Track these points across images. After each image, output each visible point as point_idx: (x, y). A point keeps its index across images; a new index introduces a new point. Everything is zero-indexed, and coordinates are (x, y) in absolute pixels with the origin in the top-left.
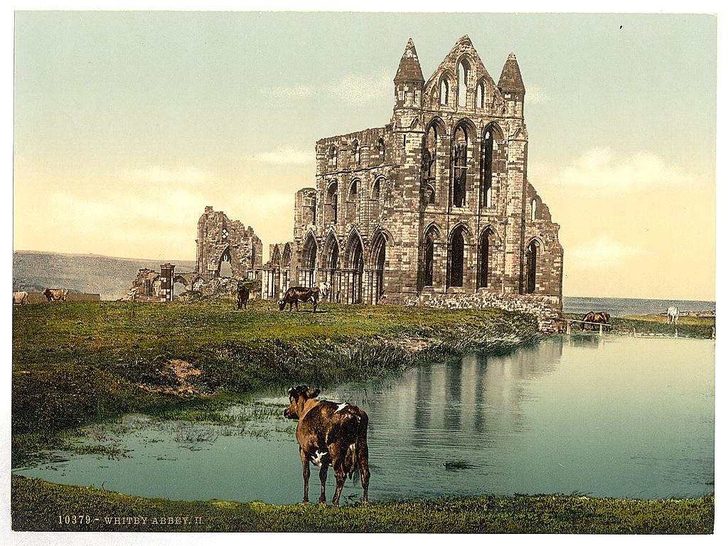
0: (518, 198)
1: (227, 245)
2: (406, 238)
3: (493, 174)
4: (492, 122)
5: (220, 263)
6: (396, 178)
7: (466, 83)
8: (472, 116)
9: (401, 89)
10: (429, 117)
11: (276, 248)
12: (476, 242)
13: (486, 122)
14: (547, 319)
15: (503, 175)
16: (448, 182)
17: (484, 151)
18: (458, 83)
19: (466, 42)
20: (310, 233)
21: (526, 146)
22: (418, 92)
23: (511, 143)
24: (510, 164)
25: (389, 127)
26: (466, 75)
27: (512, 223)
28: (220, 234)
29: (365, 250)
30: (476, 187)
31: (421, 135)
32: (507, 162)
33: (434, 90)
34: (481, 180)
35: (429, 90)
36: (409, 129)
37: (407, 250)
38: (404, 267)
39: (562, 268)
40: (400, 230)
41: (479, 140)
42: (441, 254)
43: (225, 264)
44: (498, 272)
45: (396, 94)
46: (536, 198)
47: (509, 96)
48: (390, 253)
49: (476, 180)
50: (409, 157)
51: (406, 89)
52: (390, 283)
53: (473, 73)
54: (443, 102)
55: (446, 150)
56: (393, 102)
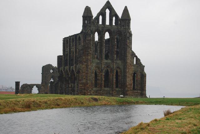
19: (108, 3)
46: (136, 57)
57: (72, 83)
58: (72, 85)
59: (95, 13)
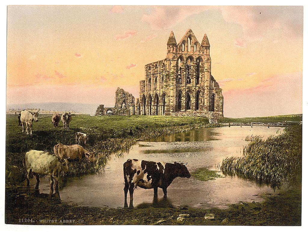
1: (124, 99)
2: (171, 95)
3: (200, 73)
4: (200, 56)
5: (122, 104)
7: (190, 44)
10: (178, 56)
14: (212, 119)
16: (185, 76)
18: (188, 44)
19: (190, 31)
21: (210, 64)
22: (175, 47)
25: (166, 59)
26: (191, 42)
27: (206, 89)
28: (123, 96)
30: (194, 77)
33: (180, 46)
34: (196, 75)
35: (178, 47)
36: (172, 60)
37: (172, 98)
38: (171, 104)
39: (223, 103)
41: (195, 62)
42: (183, 100)
43: (124, 105)
45: (168, 49)
46: (215, 81)
47: (205, 48)
48: (166, 100)
49: (194, 75)
51: (171, 47)
53: (193, 40)
54: (183, 50)
56: (166, 51)
59: (178, 41)
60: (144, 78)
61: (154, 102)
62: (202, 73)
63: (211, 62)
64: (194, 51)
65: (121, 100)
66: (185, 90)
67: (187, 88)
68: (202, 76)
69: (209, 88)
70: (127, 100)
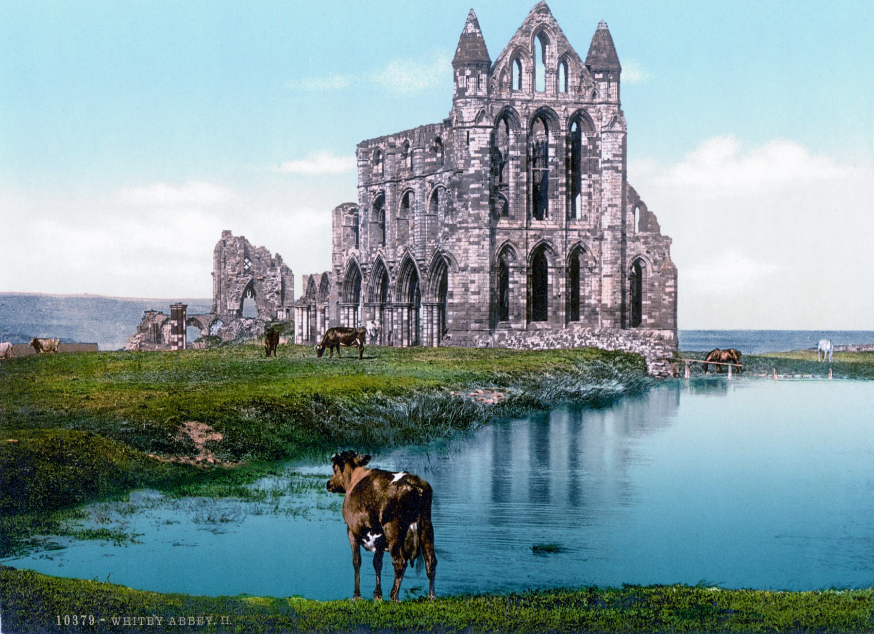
0: (616, 206)
1: (250, 277)
3: (583, 176)
4: (580, 110)
5: (242, 300)
6: (458, 186)
7: (544, 62)
8: (554, 103)
9: (462, 73)
10: (498, 107)
11: (311, 280)
12: (563, 264)
13: (572, 110)
15: (595, 177)
16: (525, 188)
17: (570, 147)
18: (534, 63)
19: (543, 9)
20: (353, 259)
21: (624, 140)
22: (484, 76)
23: (604, 135)
24: (604, 162)
25: (448, 123)
26: (544, 51)
28: (243, 265)
29: (421, 280)
30: (561, 193)
31: (489, 130)
32: (600, 161)
33: (503, 73)
34: (567, 184)
35: (497, 73)
36: (473, 124)
37: (475, 277)
38: (473, 299)
39: (676, 293)
40: (466, 251)
41: (564, 134)
42: (519, 281)
43: (249, 301)
44: (593, 301)
45: (456, 80)
47: (601, 76)
48: (453, 281)
49: (562, 185)
50: (474, 158)
51: (468, 72)
52: (456, 319)
53: (553, 48)
55: (521, 149)
56: (451, 90)
57: (402, 307)
58: (402, 313)
60: (353, 196)
61: (400, 290)
62: (590, 176)
63: (628, 131)
64: (557, 86)
65: (237, 282)
66: (527, 243)
67: (532, 237)
68: (590, 186)
69: (619, 235)
70: (262, 280)
